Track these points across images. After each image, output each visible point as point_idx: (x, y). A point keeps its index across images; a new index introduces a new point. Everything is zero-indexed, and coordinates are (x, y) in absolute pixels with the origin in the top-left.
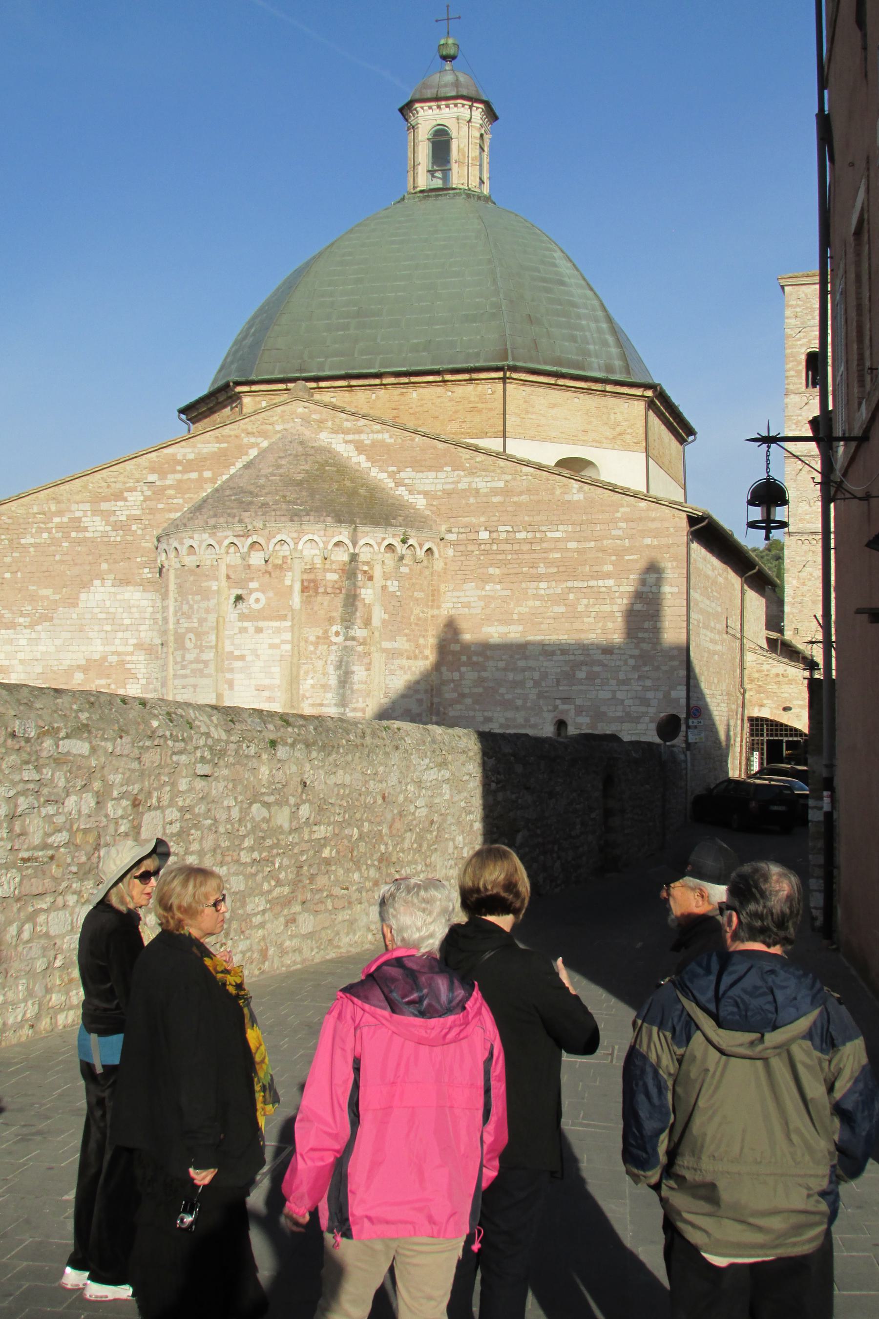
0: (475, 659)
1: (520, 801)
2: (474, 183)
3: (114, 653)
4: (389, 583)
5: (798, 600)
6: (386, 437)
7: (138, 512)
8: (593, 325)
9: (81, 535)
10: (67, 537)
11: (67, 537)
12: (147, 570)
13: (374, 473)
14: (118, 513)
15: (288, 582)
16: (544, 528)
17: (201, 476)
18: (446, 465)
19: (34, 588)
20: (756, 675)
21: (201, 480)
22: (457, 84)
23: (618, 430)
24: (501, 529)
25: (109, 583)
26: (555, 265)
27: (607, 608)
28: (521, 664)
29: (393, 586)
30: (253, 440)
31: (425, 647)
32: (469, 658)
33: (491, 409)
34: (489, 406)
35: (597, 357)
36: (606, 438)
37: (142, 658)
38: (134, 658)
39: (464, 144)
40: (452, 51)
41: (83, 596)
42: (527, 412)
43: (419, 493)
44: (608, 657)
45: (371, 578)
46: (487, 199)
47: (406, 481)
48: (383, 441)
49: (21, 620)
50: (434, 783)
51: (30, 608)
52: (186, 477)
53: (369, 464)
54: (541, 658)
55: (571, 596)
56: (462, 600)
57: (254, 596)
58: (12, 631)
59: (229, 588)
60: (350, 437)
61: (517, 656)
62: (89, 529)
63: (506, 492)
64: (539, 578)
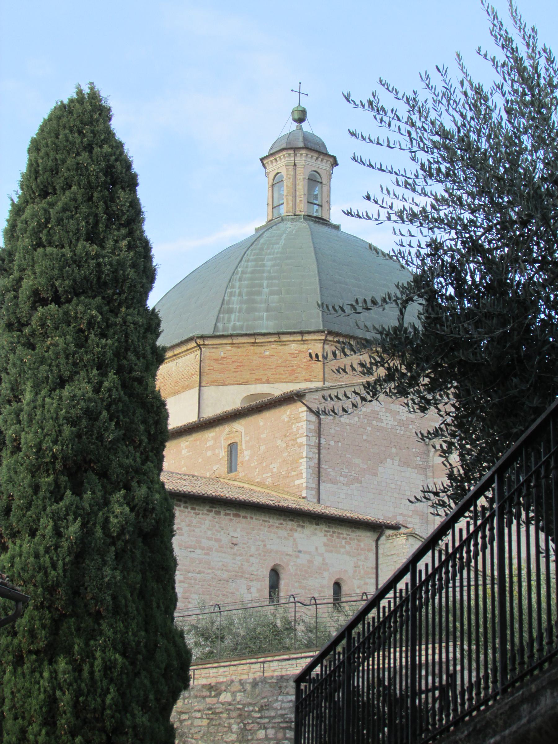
3: (401, 514)
9: (379, 424)
12: (419, 459)
14: (401, 414)
19: (350, 456)
25: (396, 463)
37: (417, 521)
38: (413, 520)
41: (381, 469)
49: (341, 479)
51: (347, 471)
58: (335, 486)
62: (384, 421)
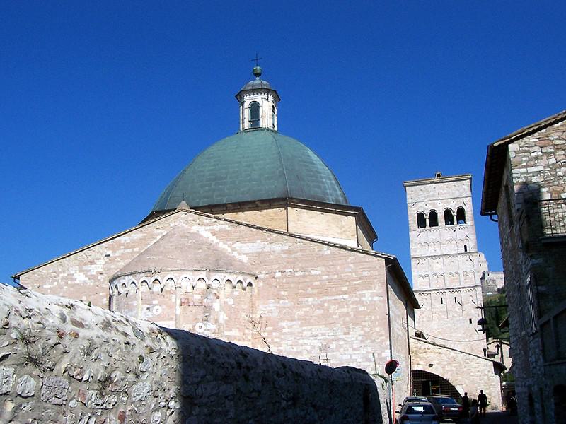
0: (275, 340)
1: (308, 417)
2: (271, 127)
4: (228, 300)
5: (421, 320)
6: (227, 226)
7: (102, 270)
8: (328, 181)
9: (73, 283)
10: (66, 284)
11: (66, 284)
13: (221, 245)
15: (174, 300)
16: (310, 269)
17: (133, 250)
18: (258, 239)
20: (415, 349)
21: (133, 252)
22: (261, 84)
23: (343, 229)
24: (287, 271)
26: (309, 156)
27: (345, 310)
28: (301, 341)
29: (231, 302)
30: (159, 231)
31: (248, 334)
32: (272, 340)
33: (280, 219)
34: (280, 217)
35: (331, 195)
36: (338, 233)
39: (265, 108)
40: (259, 72)
42: (298, 220)
43: (244, 254)
44: (347, 336)
45: (218, 298)
46: (276, 132)
47: (237, 249)
48: (225, 228)
50: (213, 398)
52: (126, 251)
53: (218, 241)
54: (311, 338)
55: (326, 304)
56: (268, 308)
57: (156, 307)
59: (143, 304)
60: (208, 228)
61: (298, 338)
63: (289, 252)
64: (309, 296)
